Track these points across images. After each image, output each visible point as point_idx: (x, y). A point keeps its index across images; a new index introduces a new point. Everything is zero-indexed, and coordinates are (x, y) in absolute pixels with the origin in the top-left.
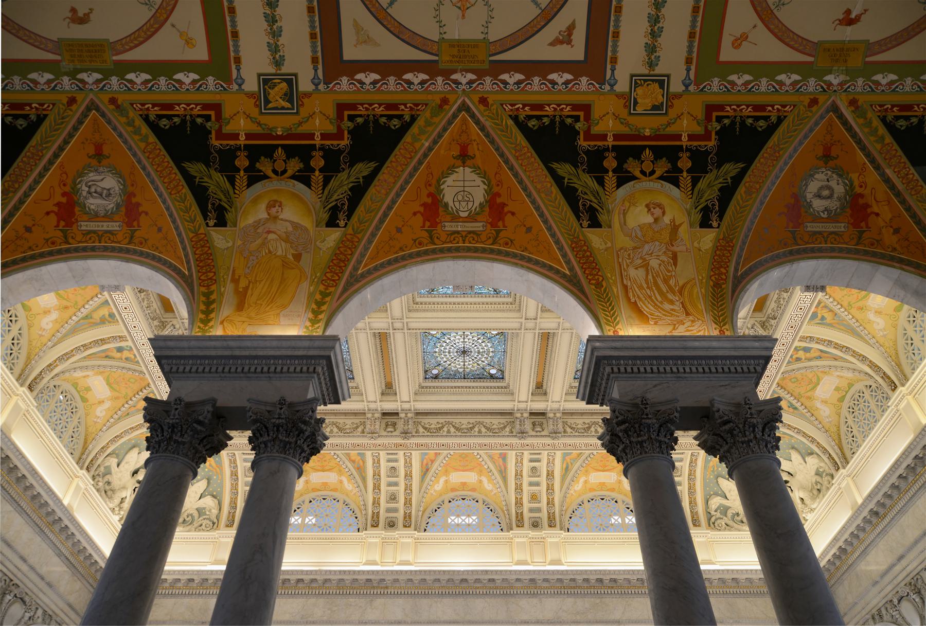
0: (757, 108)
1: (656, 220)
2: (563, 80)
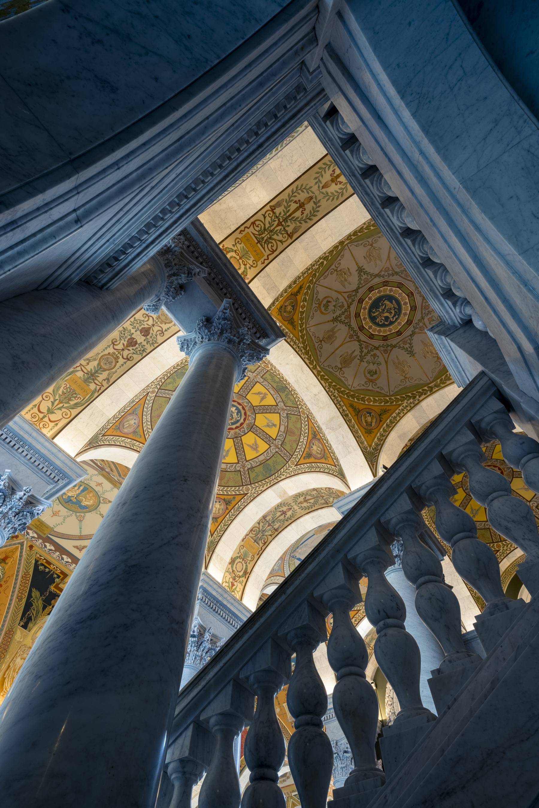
2: (67, 560)
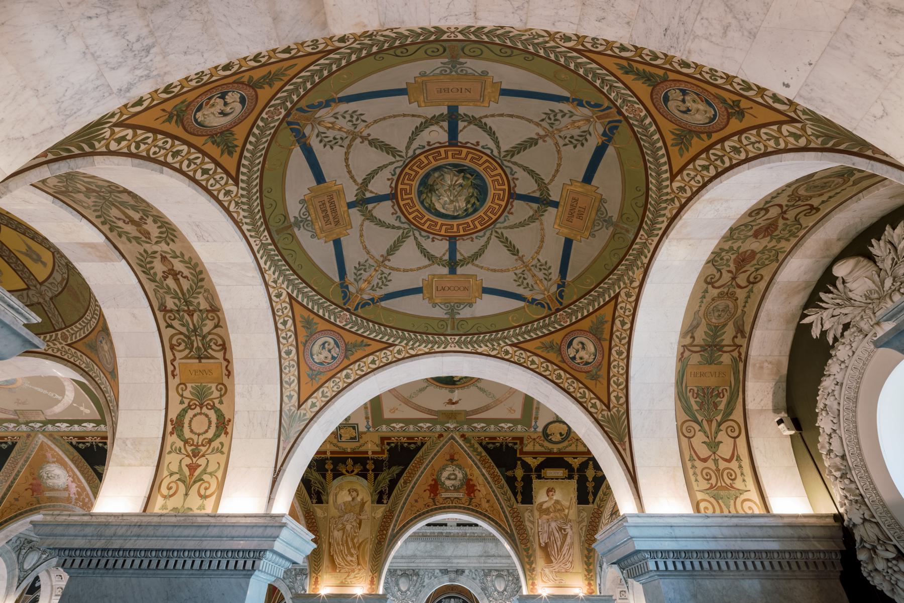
0: (409, 438)
1: (353, 499)
